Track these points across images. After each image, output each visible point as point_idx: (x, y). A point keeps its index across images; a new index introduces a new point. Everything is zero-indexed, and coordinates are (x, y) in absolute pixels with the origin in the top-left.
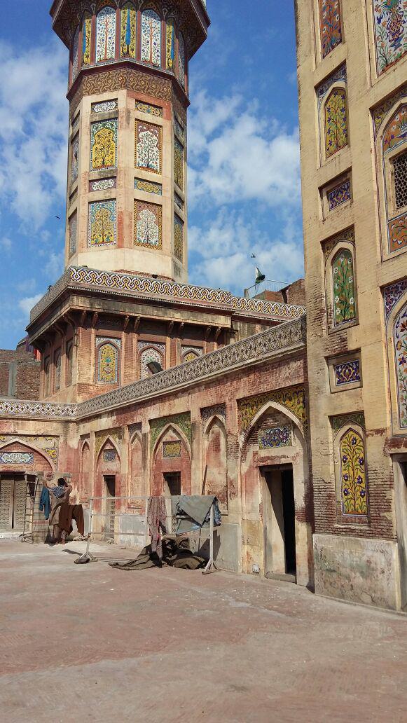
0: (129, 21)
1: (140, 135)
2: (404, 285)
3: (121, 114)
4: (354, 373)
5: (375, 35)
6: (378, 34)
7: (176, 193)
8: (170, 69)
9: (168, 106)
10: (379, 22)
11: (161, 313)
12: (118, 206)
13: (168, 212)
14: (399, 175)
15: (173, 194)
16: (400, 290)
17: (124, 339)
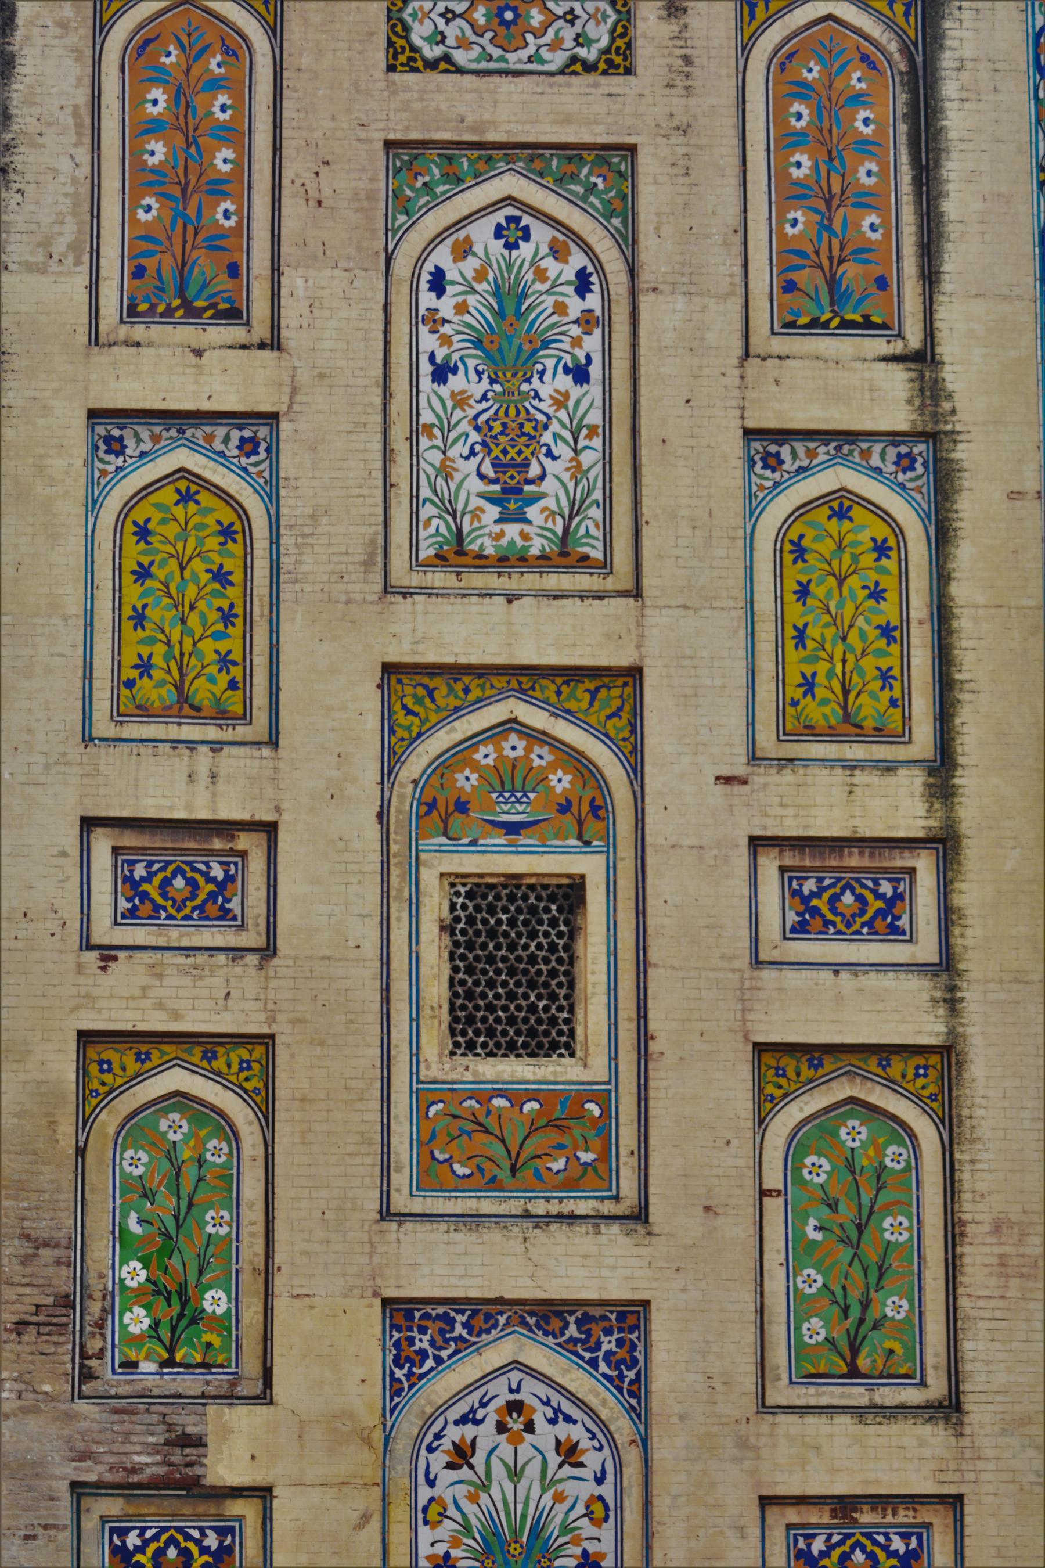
6: (427, 417)
16: (459, 1330)
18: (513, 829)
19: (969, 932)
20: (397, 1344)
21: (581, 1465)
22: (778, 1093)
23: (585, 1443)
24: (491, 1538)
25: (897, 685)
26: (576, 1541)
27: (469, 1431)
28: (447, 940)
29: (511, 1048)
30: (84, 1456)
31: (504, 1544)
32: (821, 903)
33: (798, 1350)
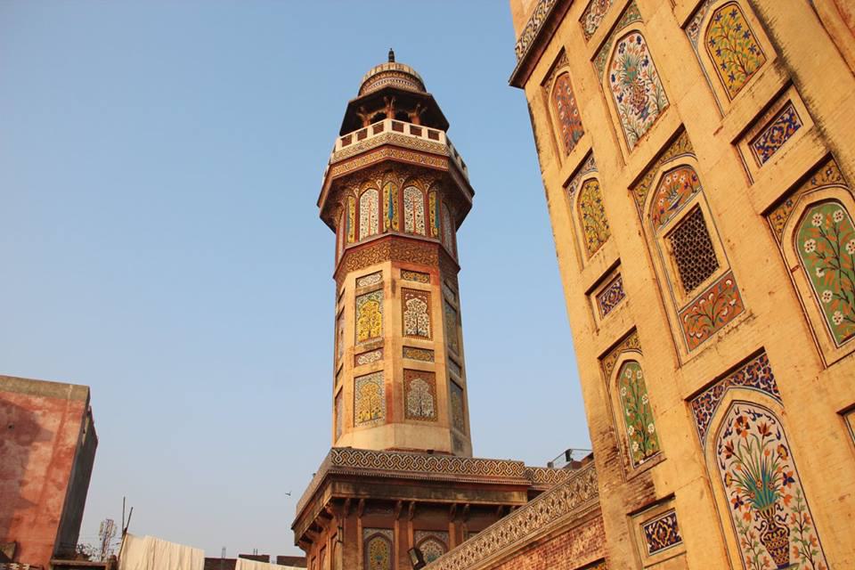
0: (391, 199)
1: (407, 303)
2: (718, 391)
3: (386, 285)
4: (671, 532)
5: (618, 114)
6: (621, 113)
7: (450, 358)
8: (435, 237)
9: (435, 270)
10: (620, 99)
11: (439, 495)
12: (386, 377)
13: (442, 379)
14: (680, 253)
15: (447, 359)
16: (713, 398)
17: (397, 530)
18: (676, 206)
19: (815, 102)
20: (698, 416)
21: (770, 434)
22: (781, 227)
23: (769, 423)
24: (750, 483)
25: (757, 47)
26: (779, 471)
27: (729, 438)
28: (673, 257)
29: (702, 279)
30: (627, 503)
31: (754, 483)
32: (769, 144)
33: (833, 331)
